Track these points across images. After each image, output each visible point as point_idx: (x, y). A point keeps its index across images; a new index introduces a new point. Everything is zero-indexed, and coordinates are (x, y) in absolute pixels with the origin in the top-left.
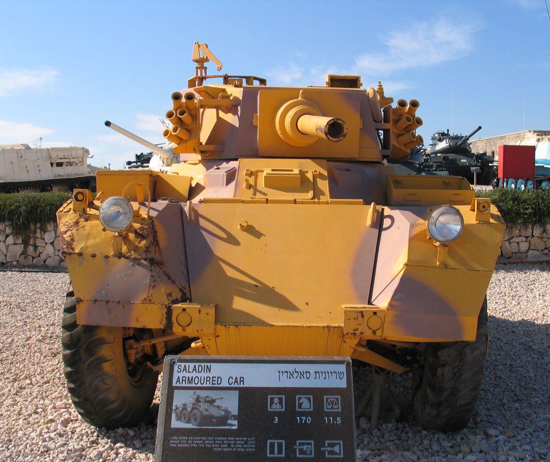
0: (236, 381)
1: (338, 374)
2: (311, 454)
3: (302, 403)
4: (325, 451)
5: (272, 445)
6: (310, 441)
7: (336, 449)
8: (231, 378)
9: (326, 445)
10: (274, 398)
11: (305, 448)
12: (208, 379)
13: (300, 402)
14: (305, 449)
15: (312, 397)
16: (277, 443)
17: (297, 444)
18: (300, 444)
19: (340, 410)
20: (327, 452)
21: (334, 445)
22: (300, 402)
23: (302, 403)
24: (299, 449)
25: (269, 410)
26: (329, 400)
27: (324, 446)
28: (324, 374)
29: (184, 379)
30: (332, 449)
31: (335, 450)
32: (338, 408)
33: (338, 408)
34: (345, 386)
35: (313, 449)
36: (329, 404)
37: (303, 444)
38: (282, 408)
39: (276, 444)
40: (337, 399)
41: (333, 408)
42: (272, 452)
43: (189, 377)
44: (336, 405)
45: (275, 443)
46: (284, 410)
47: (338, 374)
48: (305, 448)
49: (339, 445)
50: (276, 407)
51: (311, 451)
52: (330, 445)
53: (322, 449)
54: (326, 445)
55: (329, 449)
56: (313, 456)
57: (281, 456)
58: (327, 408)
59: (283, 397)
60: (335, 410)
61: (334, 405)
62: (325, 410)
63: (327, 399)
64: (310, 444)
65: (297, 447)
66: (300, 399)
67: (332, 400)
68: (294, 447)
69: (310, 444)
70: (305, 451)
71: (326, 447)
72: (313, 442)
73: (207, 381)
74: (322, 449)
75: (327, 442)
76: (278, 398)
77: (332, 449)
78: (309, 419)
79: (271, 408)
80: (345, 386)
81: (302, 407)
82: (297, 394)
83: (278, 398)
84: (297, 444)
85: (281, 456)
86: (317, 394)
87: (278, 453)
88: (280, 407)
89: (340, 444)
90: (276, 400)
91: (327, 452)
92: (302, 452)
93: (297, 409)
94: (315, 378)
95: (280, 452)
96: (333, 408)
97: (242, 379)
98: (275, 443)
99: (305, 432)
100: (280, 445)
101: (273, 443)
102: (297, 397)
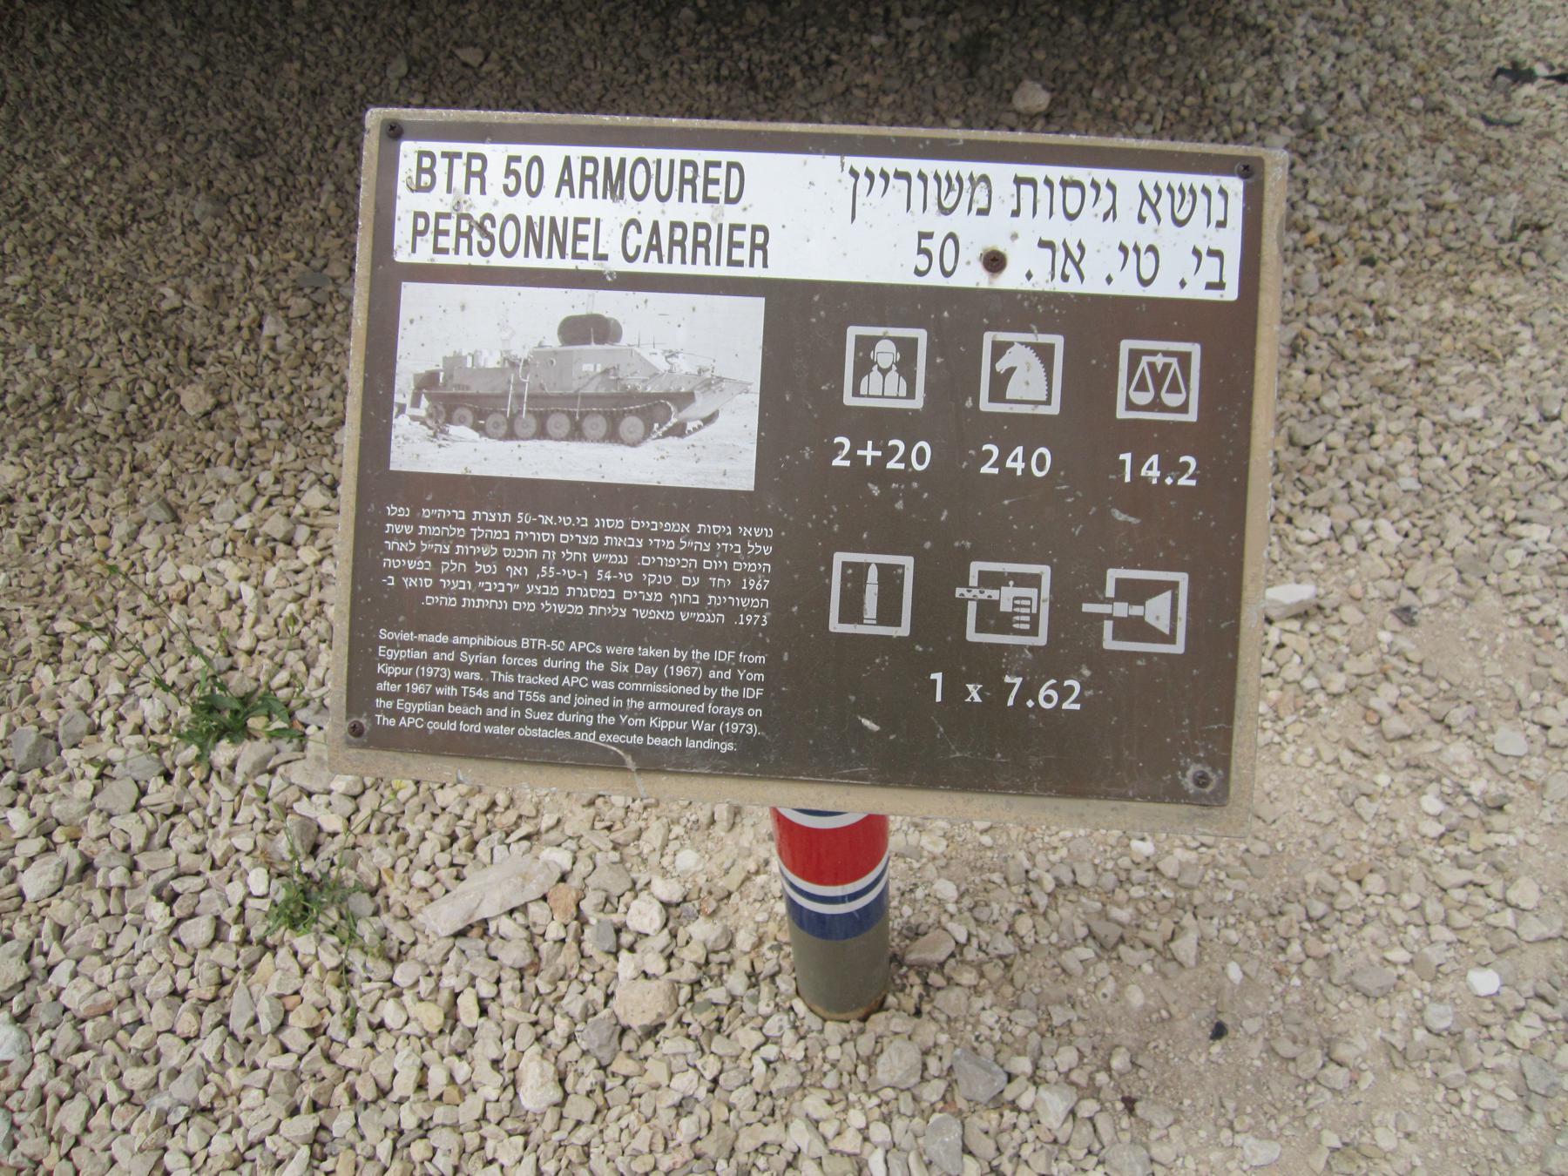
2: (1034, 631)
3: (1011, 371)
4: (1101, 617)
7: (1156, 611)
8: (633, 229)
9: (1110, 591)
10: (878, 339)
13: (1001, 366)
14: (1006, 607)
15: (1058, 341)
16: (880, 567)
17: (973, 581)
18: (988, 580)
19: (1192, 416)
20: (1108, 626)
21: (1156, 588)
22: (1001, 366)
23: (1011, 371)
24: (981, 603)
25: (849, 400)
30: (1136, 611)
31: (1150, 619)
35: (1045, 608)
36: (1142, 387)
38: (911, 394)
39: (873, 575)
40: (1184, 359)
42: (852, 612)
44: (1174, 388)
46: (918, 403)
48: (1006, 597)
50: (883, 389)
51: (1035, 620)
53: (1087, 608)
54: (1110, 591)
55: (1121, 609)
56: (1041, 640)
58: (1129, 402)
62: (1122, 413)
63: (1135, 356)
64: (1034, 581)
65: (971, 594)
66: (999, 350)
67: (1159, 361)
68: (959, 591)
69: (1034, 581)
70: (1008, 616)
71: (1109, 601)
72: (1045, 571)
74: (1087, 608)
75: (1113, 575)
76: (899, 342)
77: (1136, 611)
78: (1041, 458)
79: (856, 393)
80: (1231, 293)
82: (989, 329)
83: (899, 342)
84: (973, 581)
86: (1093, 328)
87: (881, 620)
88: (903, 393)
89: (1174, 586)
90: (886, 354)
91: (1108, 626)
92: (991, 617)
95: (888, 614)
96: (1157, 405)
99: (1010, 520)
102: (988, 338)
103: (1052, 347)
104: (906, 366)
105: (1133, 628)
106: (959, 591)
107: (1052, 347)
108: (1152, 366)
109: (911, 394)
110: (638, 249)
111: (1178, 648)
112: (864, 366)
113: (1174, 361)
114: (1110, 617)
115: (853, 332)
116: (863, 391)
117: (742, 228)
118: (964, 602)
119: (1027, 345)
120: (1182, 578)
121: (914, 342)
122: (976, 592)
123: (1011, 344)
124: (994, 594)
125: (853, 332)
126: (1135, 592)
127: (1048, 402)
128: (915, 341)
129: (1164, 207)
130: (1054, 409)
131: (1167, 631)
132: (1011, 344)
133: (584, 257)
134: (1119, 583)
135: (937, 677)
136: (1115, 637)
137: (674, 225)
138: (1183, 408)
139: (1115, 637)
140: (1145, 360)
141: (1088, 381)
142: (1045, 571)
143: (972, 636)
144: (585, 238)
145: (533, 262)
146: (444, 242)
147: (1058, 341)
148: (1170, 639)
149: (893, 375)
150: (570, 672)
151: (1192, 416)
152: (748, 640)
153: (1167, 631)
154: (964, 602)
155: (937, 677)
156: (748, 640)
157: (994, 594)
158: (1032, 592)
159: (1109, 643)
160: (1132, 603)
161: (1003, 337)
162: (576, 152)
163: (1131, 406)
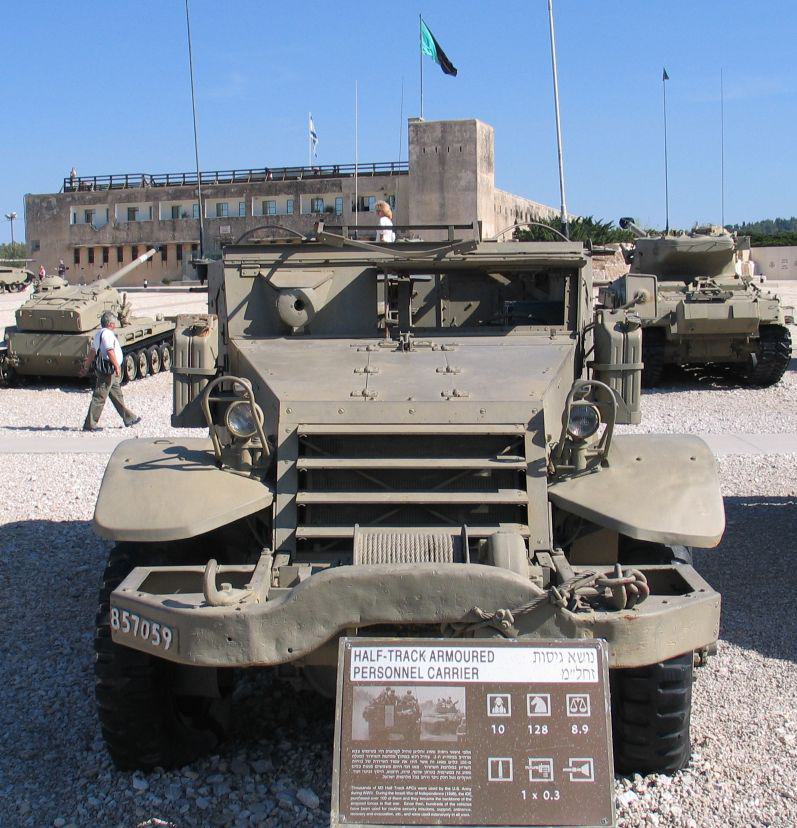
0: (439, 674)
4: (568, 773)
6: (547, 760)
7: (585, 770)
9: (571, 765)
10: (495, 698)
12: (455, 671)
14: (540, 771)
15: (549, 696)
18: (534, 764)
19: (589, 714)
20: (571, 775)
21: (583, 763)
25: (489, 714)
26: (573, 701)
27: (568, 767)
29: (447, 671)
30: (579, 770)
32: (587, 712)
33: (586, 712)
34: (596, 680)
36: (574, 707)
37: (538, 763)
38: (507, 712)
40: (585, 699)
41: (578, 712)
45: (498, 762)
46: (510, 715)
48: (540, 768)
50: (499, 711)
51: (549, 774)
52: (576, 764)
54: (571, 765)
55: (574, 770)
57: (508, 780)
61: (579, 708)
62: (568, 714)
63: (571, 699)
64: (548, 763)
65: (530, 768)
66: (532, 699)
67: (578, 700)
69: (548, 763)
72: (551, 760)
75: (571, 760)
77: (579, 770)
80: (596, 680)
85: (508, 780)
86: (558, 692)
90: (499, 701)
91: (571, 775)
92: (536, 774)
93: (529, 714)
95: (506, 775)
96: (578, 712)
97: (475, 671)
99: (543, 747)
100: (506, 764)
102: (529, 696)
103: (547, 698)
104: (505, 705)
105: (578, 775)
106: (526, 767)
109: (507, 712)
112: (493, 705)
115: (489, 696)
120: (591, 760)
124: (537, 767)
129: (576, 658)
135: (524, 792)
138: (586, 712)
142: (551, 760)
143: (531, 780)
145: (397, 679)
146: (365, 675)
150: (407, 801)
152: (466, 784)
155: (524, 792)
156: (466, 784)
157: (537, 767)
159: (572, 779)
161: (533, 695)
162: (436, 649)
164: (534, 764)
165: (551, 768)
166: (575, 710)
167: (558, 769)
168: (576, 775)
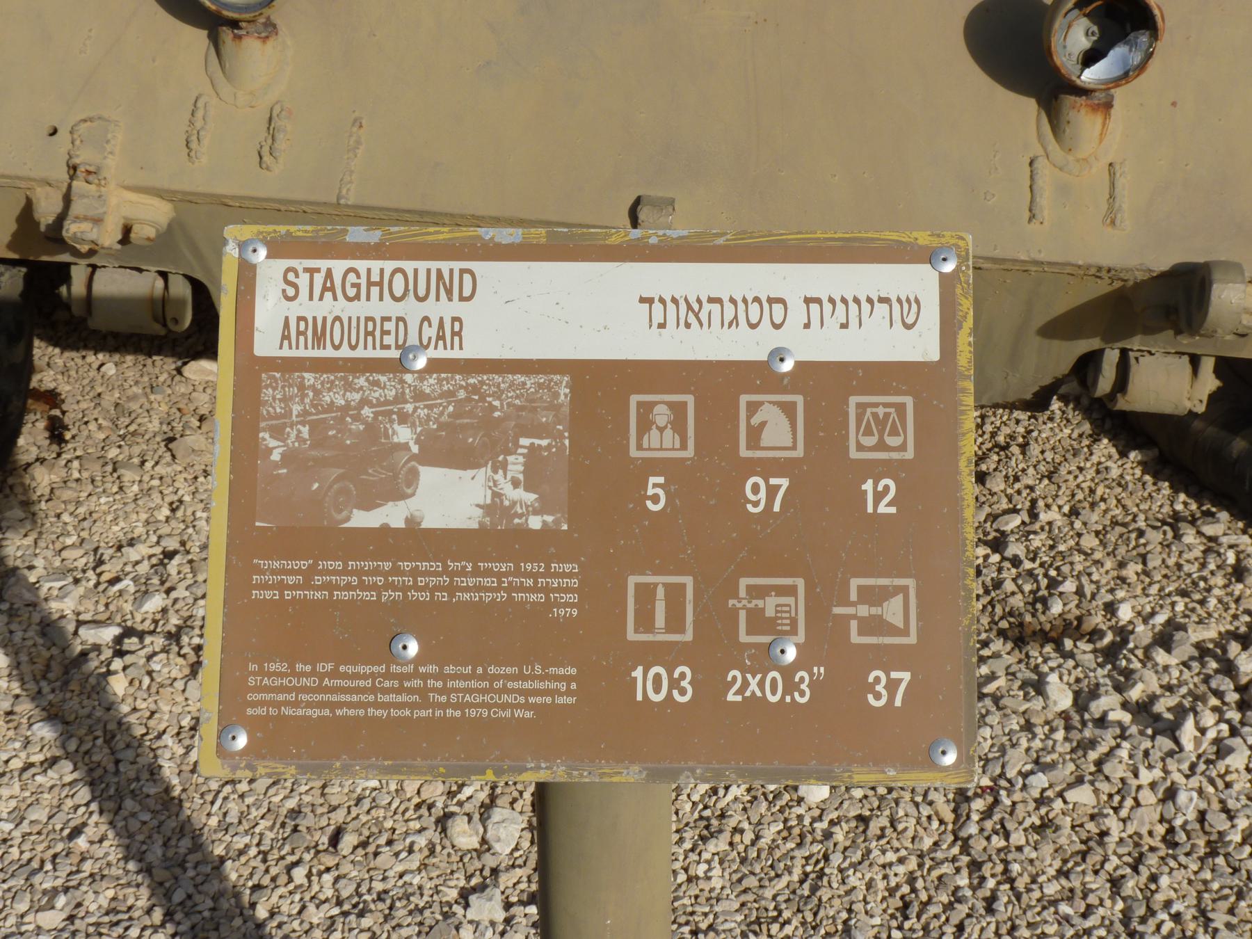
1: (896, 306)
3: (763, 424)
5: (646, 594)
7: (893, 611)
8: (426, 323)
9: (854, 597)
10: (656, 403)
11: (770, 605)
13: (755, 421)
14: (770, 612)
15: (799, 399)
16: (665, 585)
17: (742, 593)
19: (910, 454)
20: (854, 624)
22: (755, 421)
23: (763, 424)
25: (634, 453)
27: (847, 603)
28: (840, 307)
30: (875, 611)
31: (889, 618)
33: (903, 448)
36: (868, 432)
38: (684, 447)
39: (660, 592)
40: (901, 408)
42: (645, 621)
43: (315, 319)
44: (895, 432)
46: (690, 453)
47: (896, 306)
48: (770, 605)
49: (900, 597)
50: (662, 443)
51: (794, 622)
52: (867, 595)
53: (837, 610)
54: (854, 597)
55: (863, 610)
59: (690, 399)
60: (895, 455)
61: (880, 438)
62: (854, 454)
63: (861, 407)
64: (791, 591)
65: (741, 603)
66: (753, 408)
67: (881, 411)
71: (854, 604)
72: (800, 583)
73: (367, 334)
74: (837, 610)
75: (855, 583)
76: (671, 405)
77: (875, 611)
79: (639, 447)
81: (765, 442)
83: (671, 405)
84: (743, 593)
87: (669, 629)
88: (677, 445)
89: (904, 590)
90: (662, 415)
91: (854, 624)
92: (758, 622)
93: (744, 452)
94: (807, 326)
95: (676, 622)
96: (881, 446)
98: (656, 585)
100: (676, 594)
101: (647, 585)
102: (744, 399)
103: (794, 404)
104: (678, 424)
105: (874, 625)
106: (731, 602)
107: (793, 405)
108: (875, 415)
110: (430, 338)
111: (912, 639)
112: (645, 425)
113: (892, 410)
114: (854, 617)
115: (634, 399)
116: (645, 445)
117: (389, 319)
118: (735, 611)
119: (774, 403)
120: (910, 582)
121: (685, 404)
122: (744, 602)
123: (762, 403)
124: (760, 603)
125: (634, 399)
126: (872, 596)
127: (794, 448)
128: (685, 404)
130: (799, 452)
131: (902, 626)
132: (762, 403)
133: (388, 347)
134: (860, 588)
136: (860, 633)
137: (454, 319)
138: (903, 448)
139: (860, 633)
140: (869, 410)
141: (825, 428)
144: (388, 333)
147: (799, 399)
148: (905, 632)
149: (668, 433)
151: (910, 454)
153: (902, 626)
154: (735, 611)
157: (760, 603)
158: (790, 600)
159: (855, 638)
160: (872, 605)
163: (860, 448)
164: (758, 592)
165: (798, 605)
166: (870, 441)
167: (817, 611)
168: (868, 626)
